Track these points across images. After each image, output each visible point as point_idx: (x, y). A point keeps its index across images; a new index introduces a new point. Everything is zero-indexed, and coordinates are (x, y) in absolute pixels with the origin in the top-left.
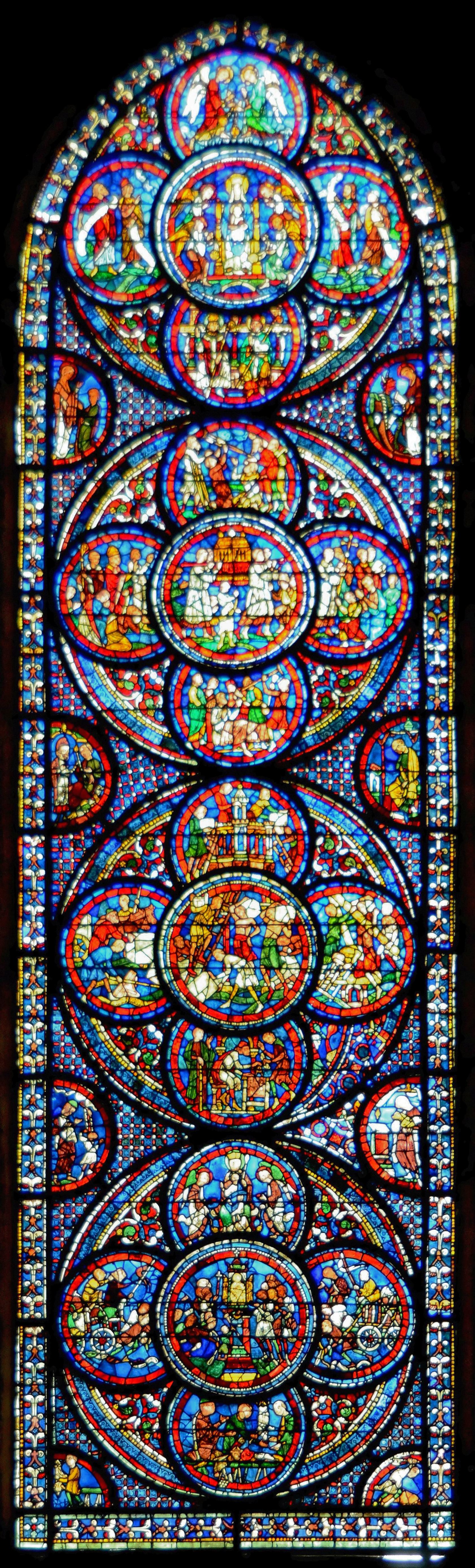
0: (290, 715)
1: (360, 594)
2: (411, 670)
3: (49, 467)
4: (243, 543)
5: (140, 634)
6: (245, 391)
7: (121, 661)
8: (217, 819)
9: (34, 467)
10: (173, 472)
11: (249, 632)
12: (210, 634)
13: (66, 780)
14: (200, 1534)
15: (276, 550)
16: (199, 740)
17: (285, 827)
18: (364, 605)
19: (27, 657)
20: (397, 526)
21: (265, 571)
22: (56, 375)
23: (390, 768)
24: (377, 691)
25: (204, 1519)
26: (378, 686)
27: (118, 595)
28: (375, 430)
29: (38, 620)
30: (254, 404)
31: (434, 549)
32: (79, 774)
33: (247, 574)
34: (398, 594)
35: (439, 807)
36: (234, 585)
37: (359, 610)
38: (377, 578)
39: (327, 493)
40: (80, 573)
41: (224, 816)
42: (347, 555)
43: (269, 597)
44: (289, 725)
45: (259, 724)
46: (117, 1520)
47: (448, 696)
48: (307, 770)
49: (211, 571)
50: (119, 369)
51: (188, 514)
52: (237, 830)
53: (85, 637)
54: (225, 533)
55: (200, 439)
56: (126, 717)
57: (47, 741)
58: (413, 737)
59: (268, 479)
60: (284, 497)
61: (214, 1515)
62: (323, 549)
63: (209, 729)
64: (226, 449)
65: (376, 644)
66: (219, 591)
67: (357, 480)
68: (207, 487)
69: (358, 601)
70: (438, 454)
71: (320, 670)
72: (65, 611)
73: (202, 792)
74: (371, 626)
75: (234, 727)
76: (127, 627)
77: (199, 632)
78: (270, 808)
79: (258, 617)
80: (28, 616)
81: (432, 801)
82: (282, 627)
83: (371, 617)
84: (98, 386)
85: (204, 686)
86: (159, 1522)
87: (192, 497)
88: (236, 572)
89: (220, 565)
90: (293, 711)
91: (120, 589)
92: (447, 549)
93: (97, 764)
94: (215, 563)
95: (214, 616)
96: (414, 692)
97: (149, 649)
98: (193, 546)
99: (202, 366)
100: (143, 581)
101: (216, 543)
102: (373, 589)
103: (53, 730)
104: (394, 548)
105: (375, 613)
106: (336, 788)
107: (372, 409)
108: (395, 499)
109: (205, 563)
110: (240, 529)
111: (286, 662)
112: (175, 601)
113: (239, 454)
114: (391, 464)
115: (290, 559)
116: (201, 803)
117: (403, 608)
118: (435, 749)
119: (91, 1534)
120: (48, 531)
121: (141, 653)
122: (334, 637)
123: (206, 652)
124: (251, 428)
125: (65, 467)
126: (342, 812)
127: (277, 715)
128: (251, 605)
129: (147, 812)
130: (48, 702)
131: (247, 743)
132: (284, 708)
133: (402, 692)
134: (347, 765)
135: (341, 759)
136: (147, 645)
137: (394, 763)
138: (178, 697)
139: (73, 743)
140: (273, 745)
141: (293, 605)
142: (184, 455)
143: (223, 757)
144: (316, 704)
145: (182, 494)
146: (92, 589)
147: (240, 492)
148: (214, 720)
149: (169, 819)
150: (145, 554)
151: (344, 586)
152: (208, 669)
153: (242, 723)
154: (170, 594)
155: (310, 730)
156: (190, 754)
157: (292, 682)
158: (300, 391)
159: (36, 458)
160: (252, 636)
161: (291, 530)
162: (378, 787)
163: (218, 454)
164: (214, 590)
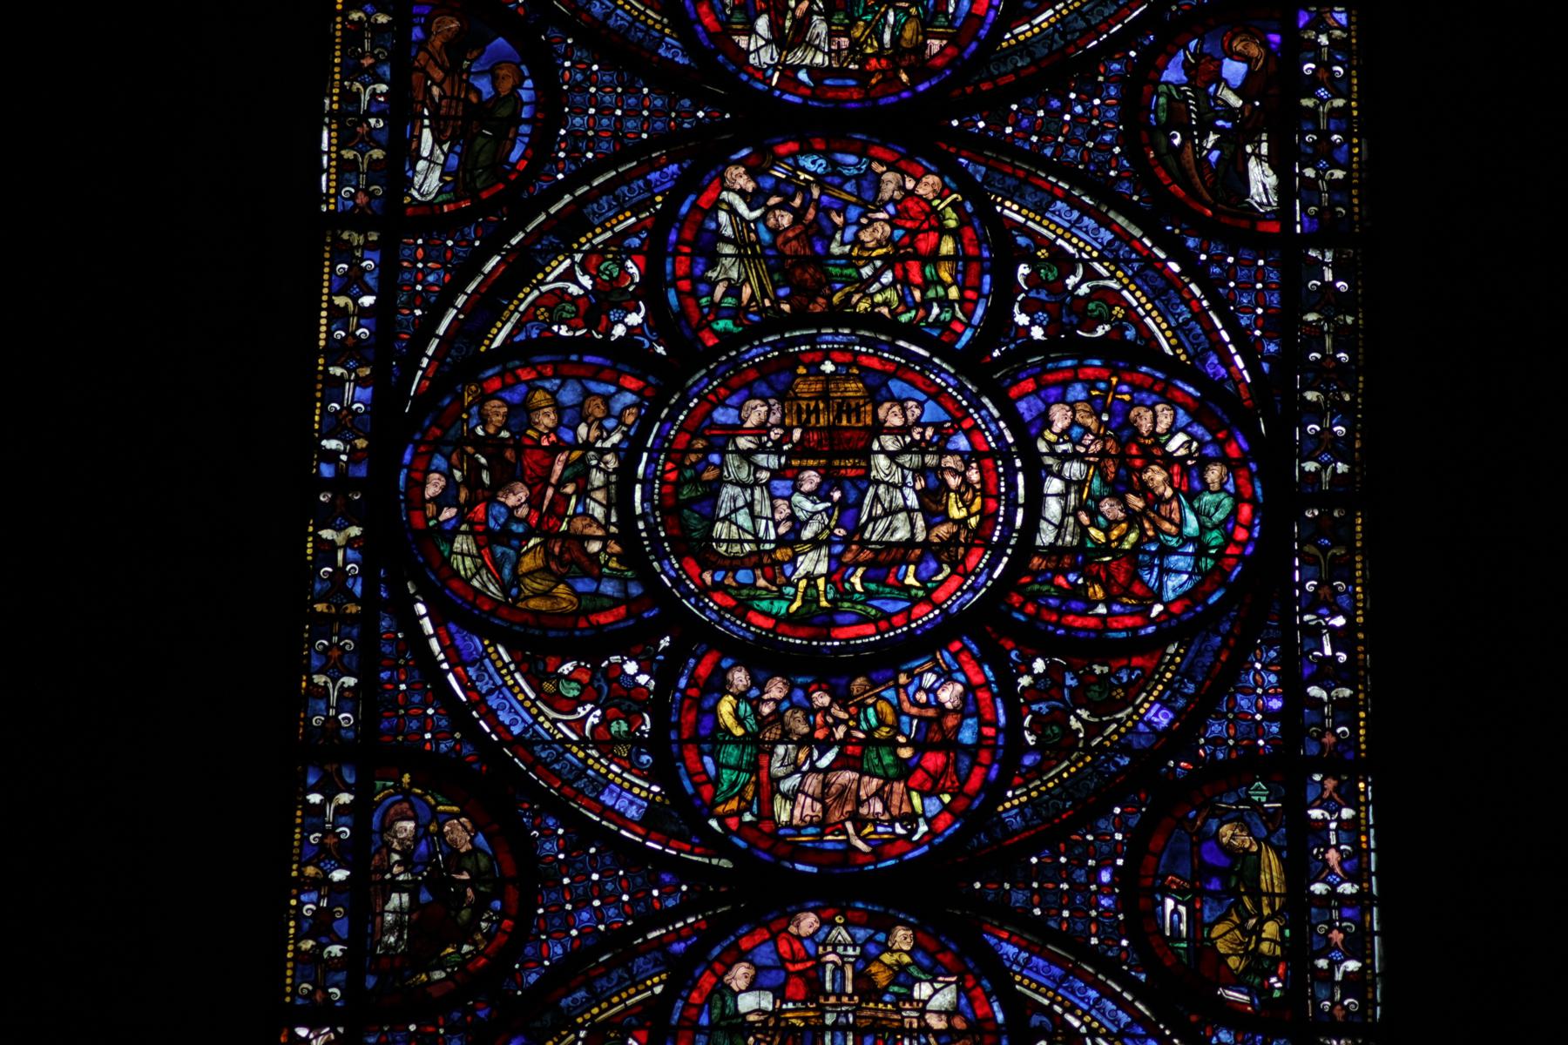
0: (965, 762)
1: (1136, 503)
2: (1263, 674)
3: (394, 217)
4: (853, 388)
5: (599, 578)
6: (863, 76)
7: (552, 634)
8: (779, 994)
9: (355, 219)
10: (688, 235)
11: (863, 579)
12: (772, 581)
13: (405, 897)
15: (930, 405)
16: (739, 813)
17: (948, 1014)
18: (1147, 525)
19: (323, 625)
20: (1227, 361)
21: (906, 449)
22: (417, 33)
23: (1215, 885)
24: (1178, 713)
26: (1181, 702)
27: (550, 492)
28: (1171, 161)
29: (350, 542)
30: (882, 102)
31: (1316, 412)
32: (439, 883)
33: (867, 454)
34: (1227, 502)
35: (1338, 976)
36: (831, 479)
37: (1133, 537)
38: (1176, 469)
39: (1058, 287)
40: (460, 443)
41: (797, 988)
42: (1105, 418)
43: (913, 501)
44: (964, 781)
45: (888, 780)
47: (1354, 729)
48: (1007, 886)
49: (778, 444)
50: (567, 25)
51: (722, 325)
52: (829, 1019)
53: (467, 581)
54: (814, 369)
55: (752, 173)
56: (559, 757)
57: (358, 813)
58: (1270, 816)
59: (916, 256)
60: (954, 293)
62: (1048, 406)
63: (766, 789)
64: (816, 193)
65: (1175, 609)
66: (796, 489)
67: (1128, 261)
68: (771, 271)
69: (1133, 518)
70: (1322, 210)
71: (1039, 666)
72: (418, 522)
73: (744, 929)
74: (1165, 571)
75: (826, 785)
76: (569, 558)
77: (743, 576)
78: (913, 970)
79: (890, 545)
80: (327, 534)
81: (1322, 963)
82: (947, 570)
83: (1165, 551)
84: (518, 59)
85: (754, 693)
87: (734, 290)
88: (839, 454)
89: (797, 434)
90: (972, 751)
91: (553, 480)
92: (1346, 412)
93: (483, 862)
94: (788, 431)
95: (781, 541)
96: (1270, 715)
97: (622, 610)
98: (733, 392)
99: (762, 24)
100: (612, 462)
101: (790, 385)
102: (1169, 493)
103: (379, 784)
104: (1215, 408)
105: (1173, 542)
106: (1080, 927)
107: (1163, 116)
108: (1219, 306)
109: (762, 429)
110: (847, 358)
111: (956, 646)
112: (689, 512)
113: (848, 203)
114: (1208, 232)
115: (967, 424)
116: (742, 957)
117: (1241, 534)
118: (1328, 846)
120: (386, 354)
121: (603, 619)
122: (1076, 592)
123: (760, 620)
124: (877, 151)
125: (429, 218)
126: (1093, 983)
127: (933, 761)
128: (873, 519)
129: (607, 975)
130: (367, 722)
131: (860, 822)
132: (950, 744)
133: (1242, 715)
134: (1105, 877)
135: (1091, 862)
136: (617, 603)
137: (1224, 874)
138: (690, 717)
139: (425, 815)
140: (923, 828)
141: (973, 521)
142: (717, 204)
143: (800, 853)
144: (1030, 739)
145: (713, 284)
146: (485, 476)
147: (848, 281)
148: (777, 769)
149: (658, 990)
150: (617, 407)
151: (1096, 483)
152: (765, 658)
153: (848, 776)
154: (677, 492)
155: (1014, 798)
156: (718, 845)
157: (969, 687)
158: (991, 78)
159: (362, 199)
160: (873, 586)
161: (970, 363)
162: (1183, 927)
163: (797, 202)
164: (782, 486)
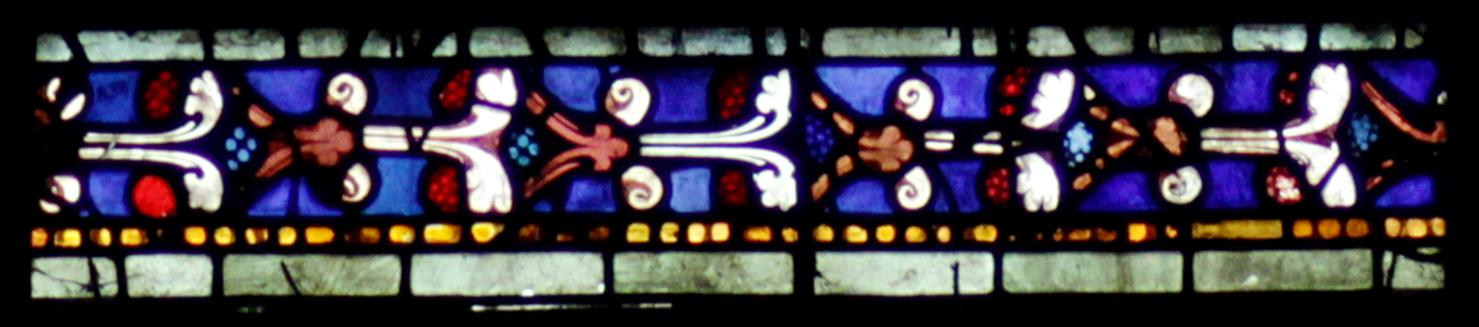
14: (1185, 186)
25: (1218, 67)
46: (529, 74)
61: (1293, 41)
86: (860, 88)
119: (327, 181)
